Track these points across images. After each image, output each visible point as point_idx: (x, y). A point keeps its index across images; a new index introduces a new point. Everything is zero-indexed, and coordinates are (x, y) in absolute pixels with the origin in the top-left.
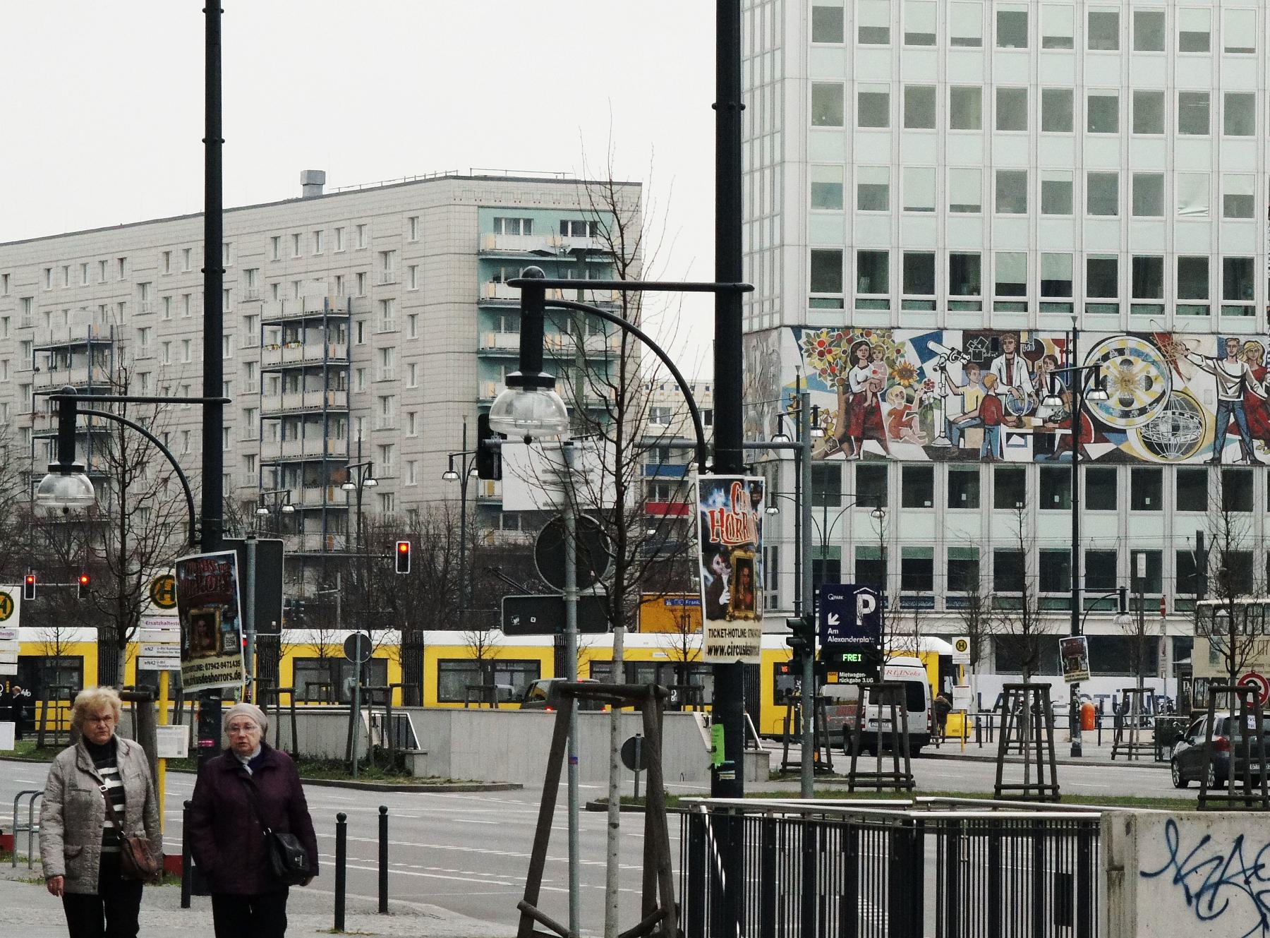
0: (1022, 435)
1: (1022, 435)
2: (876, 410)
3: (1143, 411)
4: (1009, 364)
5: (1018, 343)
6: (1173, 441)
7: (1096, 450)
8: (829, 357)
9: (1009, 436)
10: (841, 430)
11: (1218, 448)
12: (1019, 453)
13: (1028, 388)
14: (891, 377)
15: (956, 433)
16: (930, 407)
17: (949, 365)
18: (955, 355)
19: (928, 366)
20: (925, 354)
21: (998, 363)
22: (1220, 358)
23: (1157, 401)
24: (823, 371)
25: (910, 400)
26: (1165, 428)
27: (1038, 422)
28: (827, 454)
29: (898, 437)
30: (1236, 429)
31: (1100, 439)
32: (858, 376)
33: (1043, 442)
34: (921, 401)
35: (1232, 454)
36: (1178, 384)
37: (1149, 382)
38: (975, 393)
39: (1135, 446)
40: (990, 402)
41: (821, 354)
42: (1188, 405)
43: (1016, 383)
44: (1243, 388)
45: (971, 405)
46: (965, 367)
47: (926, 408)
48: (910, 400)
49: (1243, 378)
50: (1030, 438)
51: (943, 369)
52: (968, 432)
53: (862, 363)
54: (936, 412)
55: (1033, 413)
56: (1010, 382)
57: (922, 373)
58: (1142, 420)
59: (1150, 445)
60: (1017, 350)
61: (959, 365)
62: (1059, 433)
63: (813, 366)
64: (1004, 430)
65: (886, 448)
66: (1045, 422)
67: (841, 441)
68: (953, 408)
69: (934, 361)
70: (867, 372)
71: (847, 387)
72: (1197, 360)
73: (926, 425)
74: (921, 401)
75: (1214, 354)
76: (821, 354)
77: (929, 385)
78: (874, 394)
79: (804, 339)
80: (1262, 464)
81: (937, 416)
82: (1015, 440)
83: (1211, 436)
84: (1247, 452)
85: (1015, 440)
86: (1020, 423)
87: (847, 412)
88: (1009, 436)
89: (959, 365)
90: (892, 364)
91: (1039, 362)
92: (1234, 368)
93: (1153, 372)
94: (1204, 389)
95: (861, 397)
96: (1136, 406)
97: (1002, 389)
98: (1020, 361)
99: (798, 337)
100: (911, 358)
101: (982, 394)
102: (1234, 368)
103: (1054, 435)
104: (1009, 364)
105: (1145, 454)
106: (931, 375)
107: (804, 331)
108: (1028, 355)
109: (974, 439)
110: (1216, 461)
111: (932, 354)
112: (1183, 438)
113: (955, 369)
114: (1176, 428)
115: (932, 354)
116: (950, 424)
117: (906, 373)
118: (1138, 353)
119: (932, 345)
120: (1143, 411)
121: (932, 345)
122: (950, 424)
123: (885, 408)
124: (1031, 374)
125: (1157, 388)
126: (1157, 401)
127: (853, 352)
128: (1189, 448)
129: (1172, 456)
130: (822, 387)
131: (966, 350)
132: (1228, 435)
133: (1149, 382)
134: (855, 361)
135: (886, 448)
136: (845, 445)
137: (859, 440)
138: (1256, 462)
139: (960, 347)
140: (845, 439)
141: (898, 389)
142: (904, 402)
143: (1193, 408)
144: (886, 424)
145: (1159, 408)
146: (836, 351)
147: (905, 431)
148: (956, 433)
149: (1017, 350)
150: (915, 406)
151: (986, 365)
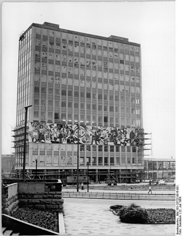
0: (65, 140)
1: (65, 140)
2: (43, 135)
3: (82, 137)
4: (63, 129)
5: (65, 126)
6: (86, 141)
8: (36, 127)
9: (63, 140)
10: (38, 138)
13: (66, 133)
14: (46, 130)
16: (52, 135)
17: (55, 129)
18: (56, 128)
19: (52, 129)
20: (51, 127)
21: (62, 129)
22: (92, 129)
23: (84, 135)
24: (36, 129)
25: (49, 134)
26: (85, 139)
27: (67, 138)
28: (36, 142)
29: (47, 140)
30: (94, 139)
31: (76, 141)
32: (41, 130)
34: (50, 134)
36: (87, 133)
37: (83, 133)
38: (58, 133)
39: (81, 142)
40: (61, 135)
41: (35, 127)
42: (88, 136)
43: (64, 132)
44: (95, 134)
45: (58, 135)
46: (57, 129)
47: (51, 135)
48: (49, 134)
49: (95, 132)
50: (66, 140)
51: (54, 130)
52: (57, 139)
53: (42, 128)
54: (53, 136)
55: (67, 136)
56: (64, 132)
57: (50, 130)
58: (82, 138)
59: (83, 142)
61: (56, 129)
62: (70, 140)
64: (63, 139)
65: (45, 141)
66: (69, 138)
67: (38, 140)
68: (55, 136)
69: (52, 128)
70: (41, 130)
71: (39, 131)
72: (89, 129)
73: (51, 138)
74: (50, 134)
75: (92, 129)
76: (35, 127)
77: (52, 132)
78: (43, 133)
79: (33, 124)
80: (98, 144)
81: (53, 137)
82: (64, 140)
83: (91, 141)
84: (96, 143)
85: (64, 140)
86: (65, 138)
87: (39, 135)
88: (63, 140)
89: (56, 129)
90: (46, 128)
91: (68, 129)
92: (94, 131)
93: (84, 131)
94: (89, 133)
95: (41, 133)
96: (81, 136)
97: (62, 133)
98: (65, 129)
99: (32, 124)
100: (49, 128)
101: (59, 133)
102: (94, 131)
103: (69, 140)
104: (63, 129)
106: (52, 130)
107: (33, 123)
108: (66, 128)
109: (58, 140)
110: (92, 144)
111: (52, 127)
112: (88, 141)
113: (56, 130)
114: (87, 139)
115: (52, 127)
116: (55, 138)
117: (48, 130)
118: (82, 128)
119: (52, 126)
120: (82, 137)
121: (52, 126)
122: (55, 138)
124: (67, 131)
125: (84, 133)
126: (84, 135)
127: (40, 127)
129: (86, 144)
131: (57, 127)
132: (94, 140)
133: (83, 133)
134: (40, 128)
135: (45, 141)
136: (39, 141)
137: (41, 140)
138: (97, 144)
139: (56, 126)
141: (47, 132)
142: (48, 134)
143: (89, 136)
144: (45, 137)
145: (84, 136)
146: (37, 126)
147: (48, 139)
148: (56, 139)
149: (65, 127)
150: (49, 135)
151: (60, 129)
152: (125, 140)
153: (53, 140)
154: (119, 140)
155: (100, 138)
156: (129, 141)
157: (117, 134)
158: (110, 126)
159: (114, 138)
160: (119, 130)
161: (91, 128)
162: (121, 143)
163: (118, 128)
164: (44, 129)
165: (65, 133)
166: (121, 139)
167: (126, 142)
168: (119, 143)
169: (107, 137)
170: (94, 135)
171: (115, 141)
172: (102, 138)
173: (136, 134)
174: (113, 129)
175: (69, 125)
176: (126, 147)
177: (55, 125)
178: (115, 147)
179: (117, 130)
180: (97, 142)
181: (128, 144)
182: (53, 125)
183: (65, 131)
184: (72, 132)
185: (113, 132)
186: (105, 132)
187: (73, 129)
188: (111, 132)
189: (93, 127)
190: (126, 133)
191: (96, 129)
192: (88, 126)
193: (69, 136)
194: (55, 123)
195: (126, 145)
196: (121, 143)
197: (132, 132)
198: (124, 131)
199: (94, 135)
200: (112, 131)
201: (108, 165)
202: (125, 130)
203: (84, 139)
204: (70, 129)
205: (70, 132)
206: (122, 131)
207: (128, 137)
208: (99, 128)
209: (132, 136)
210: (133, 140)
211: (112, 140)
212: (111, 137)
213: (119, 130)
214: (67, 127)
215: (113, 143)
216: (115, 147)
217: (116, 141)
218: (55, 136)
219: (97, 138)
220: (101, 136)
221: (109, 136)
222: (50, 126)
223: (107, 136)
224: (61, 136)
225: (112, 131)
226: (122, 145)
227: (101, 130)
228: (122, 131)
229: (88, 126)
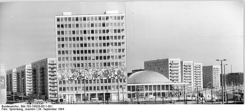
7: (82, 79)
11: (92, 78)
12: (76, 79)
20: (68, 72)
21: (74, 72)
26: (88, 77)
32: (62, 74)
33: (78, 78)
35: (94, 79)
38: (72, 75)
39: (85, 79)
40: (73, 75)
47: (68, 76)
59: (87, 78)
63: (59, 73)
81: (69, 77)
84: (95, 79)
92: (93, 72)
100: (67, 72)
102: (93, 72)
105: (87, 79)
109: (72, 78)
112: (90, 78)
113: (70, 73)
117: (66, 73)
123: (65, 76)
128: (90, 78)
129: (89, 79)
140: (62, 79)
151: (73, 73)
152: (114, 76)
153: (69, 79)
154: (110, 76)
155: (97, 76)
156: (117, 76)
158: (104, 68)
160: (110, 70)
161: (91, 70)
162: (111, 77)
163: (109, 69)
164: (64, 73)
166: (111, 75)
167: (114, 77)
168: (110, 77)
169: (102, 75)
170: (93, 74)
172: (99, 75)
173: (122, 71)
174: (106, 70)
175: (78, 70)
176: (115, 80)
177: (70, 70)
178: (108, 80)
180: (96, 78)
181: (116, 78)
182: (69, 71)
183: (76, 73)
184: (80, 74)
186: (101, 72)
187: (80, 72)
188: (105, 72)
189: (92, 70)
190: (115, 72)
191: (94, 70)
192: (89, 70)
193: (78, 76)
194: (70, 69)
195: (115, 78)
196: (111, 77)
197: (119, 70)
198: (113, 70)
199: (93, 74)
202: (114, 70)
205: (79, 74)
206: (112, 70)
207: (116, 73)
208: (97, 70)
209: (119, 73)
210: (120, 75)
212: (105, 74)
213: (110, 70)
216: (108, 80)
218: (71, 77)
219: (95, 76)
220: (98, 75)
221: (103, 74)
222: (67, 71)
223: (102, 74)
224: (73, 77)
225: (105, 71)
226: (112, 78)
228: (112, 70)
229: (89, 70)
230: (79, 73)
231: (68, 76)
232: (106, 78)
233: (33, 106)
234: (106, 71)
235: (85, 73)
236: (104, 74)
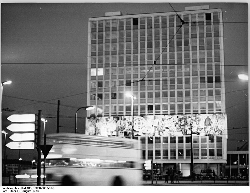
0: (122, 133)
1: (122, 133)
4: (120, 121)
9: (120, 133)
15: (112, 132)
21: (119, 121)
24: (92, 124)
50: (124, 133)
55: (124, 129)
60: (122, 119)
71: (95, 126)
85: (121, 133)
86: (122, 131)
88: (120, 133)
101: (116, 126)
104: (120, 121)
130: (92, 126)
140: (95, 134)
149: (122, 119)
151: (117, 122)
157: (186, 122)
159: (182, 127)
165: (122, 125)
171: (184, 130)
179: (187, 117)
185: (181, 120)
188: (179, 120)
200: (180, 119)
201: (175, 158)
203: (144, 130)
204: (127, 120)
209: (208, 123)
211: (181, 129)
214: (124, 119)
215: (182, 133)
217: (185, 131)
227: (166, 119)
230: (128, 122)
231: (107, 129)
232: (181, 134)
233: (34, 188)
234: (182, 118)
235: (139, 124)
236: (177, 125)
